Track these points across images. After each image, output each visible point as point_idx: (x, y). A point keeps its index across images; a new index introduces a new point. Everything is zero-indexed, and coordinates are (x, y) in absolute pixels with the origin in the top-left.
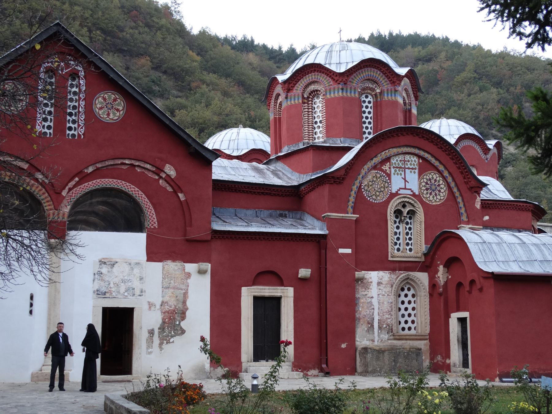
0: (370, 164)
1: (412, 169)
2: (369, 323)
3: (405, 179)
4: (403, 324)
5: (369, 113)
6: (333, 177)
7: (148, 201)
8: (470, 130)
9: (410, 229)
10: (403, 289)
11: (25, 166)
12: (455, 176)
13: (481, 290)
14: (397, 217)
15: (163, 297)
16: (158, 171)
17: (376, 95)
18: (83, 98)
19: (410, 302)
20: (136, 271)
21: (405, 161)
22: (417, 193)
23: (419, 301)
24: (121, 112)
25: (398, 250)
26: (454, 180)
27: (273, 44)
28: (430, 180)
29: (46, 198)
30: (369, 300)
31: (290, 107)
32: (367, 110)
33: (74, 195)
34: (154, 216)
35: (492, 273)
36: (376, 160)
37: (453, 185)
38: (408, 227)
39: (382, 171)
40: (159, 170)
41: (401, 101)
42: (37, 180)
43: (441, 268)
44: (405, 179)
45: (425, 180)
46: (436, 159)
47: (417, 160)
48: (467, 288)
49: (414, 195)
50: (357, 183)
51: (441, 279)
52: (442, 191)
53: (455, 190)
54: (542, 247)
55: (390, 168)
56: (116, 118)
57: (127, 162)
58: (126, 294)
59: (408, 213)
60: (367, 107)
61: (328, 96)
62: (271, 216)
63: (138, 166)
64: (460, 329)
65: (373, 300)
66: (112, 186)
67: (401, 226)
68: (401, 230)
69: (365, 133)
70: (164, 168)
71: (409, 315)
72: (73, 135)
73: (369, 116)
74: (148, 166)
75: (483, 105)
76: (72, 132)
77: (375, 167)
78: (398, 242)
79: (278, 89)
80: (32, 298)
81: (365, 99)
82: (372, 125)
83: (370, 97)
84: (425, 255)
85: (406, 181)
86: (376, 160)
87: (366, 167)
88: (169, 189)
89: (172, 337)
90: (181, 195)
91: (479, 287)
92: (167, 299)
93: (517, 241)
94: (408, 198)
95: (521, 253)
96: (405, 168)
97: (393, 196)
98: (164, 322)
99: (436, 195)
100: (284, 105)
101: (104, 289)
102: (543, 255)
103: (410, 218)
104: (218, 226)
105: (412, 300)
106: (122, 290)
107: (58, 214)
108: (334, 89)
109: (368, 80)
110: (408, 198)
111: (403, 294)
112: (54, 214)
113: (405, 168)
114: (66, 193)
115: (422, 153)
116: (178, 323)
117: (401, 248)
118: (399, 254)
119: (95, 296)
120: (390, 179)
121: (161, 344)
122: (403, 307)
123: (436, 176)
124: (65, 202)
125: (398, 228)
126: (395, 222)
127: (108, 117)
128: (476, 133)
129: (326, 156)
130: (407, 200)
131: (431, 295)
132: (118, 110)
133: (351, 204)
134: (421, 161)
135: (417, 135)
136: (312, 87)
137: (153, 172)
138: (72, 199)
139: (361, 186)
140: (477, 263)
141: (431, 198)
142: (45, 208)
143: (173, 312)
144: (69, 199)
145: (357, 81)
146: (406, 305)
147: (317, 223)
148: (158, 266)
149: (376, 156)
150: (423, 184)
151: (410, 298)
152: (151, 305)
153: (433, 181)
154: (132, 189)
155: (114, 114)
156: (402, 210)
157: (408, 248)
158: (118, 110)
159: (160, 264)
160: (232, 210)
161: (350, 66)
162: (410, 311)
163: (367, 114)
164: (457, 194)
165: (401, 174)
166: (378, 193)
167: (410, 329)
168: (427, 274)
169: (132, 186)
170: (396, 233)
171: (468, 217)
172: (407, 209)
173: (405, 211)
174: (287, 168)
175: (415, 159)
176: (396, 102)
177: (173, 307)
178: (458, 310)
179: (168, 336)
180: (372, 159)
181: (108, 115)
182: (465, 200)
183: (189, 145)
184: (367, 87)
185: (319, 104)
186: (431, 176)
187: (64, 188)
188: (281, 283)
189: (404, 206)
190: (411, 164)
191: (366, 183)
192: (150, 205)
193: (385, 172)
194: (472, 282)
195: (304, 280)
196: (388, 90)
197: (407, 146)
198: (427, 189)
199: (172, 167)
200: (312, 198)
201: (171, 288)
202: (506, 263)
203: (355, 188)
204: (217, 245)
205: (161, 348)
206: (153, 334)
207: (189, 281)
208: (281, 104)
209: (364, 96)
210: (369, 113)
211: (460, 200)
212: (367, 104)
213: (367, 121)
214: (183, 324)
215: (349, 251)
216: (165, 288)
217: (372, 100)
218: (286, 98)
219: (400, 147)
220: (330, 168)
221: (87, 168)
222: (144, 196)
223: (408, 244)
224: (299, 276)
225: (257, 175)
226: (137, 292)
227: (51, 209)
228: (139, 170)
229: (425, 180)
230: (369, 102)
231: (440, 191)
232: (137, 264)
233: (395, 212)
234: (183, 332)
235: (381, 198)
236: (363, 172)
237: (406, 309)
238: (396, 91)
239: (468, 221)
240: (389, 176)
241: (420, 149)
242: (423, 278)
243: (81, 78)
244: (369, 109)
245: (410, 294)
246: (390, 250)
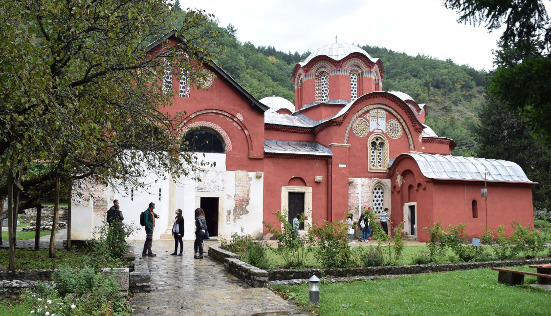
0: (357, 114)
1: (382, 117)
2: (356, 209)
3: (378, 124)
4: (375, 210)
5: (355, 85)
6: (336, 122)
9: (380, 153)
10: (376, 189)
12: (407, 122)
13: (425, 189)
14: (373, 146)
15: (236, 191)
16: (232, 117)
17: (359, 74)
19: (379, 197)
20: (220, 176)
21: (378, 113)
22: (385, 132)
23: (385, 196)
24: (211, 82)
25: (373, 166)
26: (406, 124)
28: (392, 124)
30: (356, 195)
32: (354, 83)
34: (230, 144)
35: (433, 179)
36: (361, 112)
37: (405, 127)
38: (379, 152)
39: (365, 118)
40: (233, 117)
43: (399, 177)
44: (378, 124)
45: (390, 125)
46: (396, 112)
47: (385, 112)
48: (416, 188)
49: (383, 133)
50: (350, 126)
51: (399, 183)
52: (400, 131)
53: (407, 130)
54: (460, 164)
55: (369, 117)
56: (208, 85)
57: (215, 111)
58: (214, 189)
59: (379, 144)
60: (353, 81)
61: (331, 75)
62: (297, 145)
63: (221, 114)
64: (410, 212)
65: (359, 195)
66: (206, 125)
67: (375, 152)
68: (375, 154)
69: (352, 97)
71: (379, 204)
72: (183, 96)
73: (355, 87)
74: (227, 114)
75: (407, 88)
76: (183, 94)
77: (360, 116)
78: (373, 161)
79: (300, 71)
80: (160, 191)
81: (352, 76)
82: (356, 92)
83: (355, 75)
84: (389, 169)
85: (378, 125)
86: (361, 112)
87: (355, 116)
88: (240, 128)
89: (241, 215)
90: (246, 131)
91: (423, 187)
92: (238, 193)
93: (446, 160)
94: (380, 135)
95: (448, 167)
96: (378, 117)
97: (371, 133)
98: (236, 206)
99: (396, 133)
100: (303, 81)
101: (201, 187)
102: (461, 169)
103: (380, 147)
104: (267, 150)
105: (381, 195)
106: (212, 187)
108: (334, 70)
109: (355, 65)
110: (380, 135)
111: (376, 192)
113: (378, 117)
115: (388, 108)
116: (244, 207)
117: (375, 165)
118: (374, 168)
119: (196, 190)
120: (369, 123)
121: (235, 219)
122: (375, 199)
123: (396, 122)
125: (373, 152)
126: (372, 149)
128: (412, 100)
129: (330, 110)
130: (379, 136)
131: (392, 193)
132: (209, 81)
133: (346, 138)
134: (387, 113)
135: (386, 97)
136: (321, 70)
137: (230, 117)
139: (352, 127)
140: (423, 173)
141: (393, 135)
143: (242, 200)
145: (348, 66)
146: (377, 198)
147: (326, 149)
148: (232, 173)
149: (361, 110)
150: (389, 127)
151: (380, 194)
152: (229, 196)
153: (394, 125)
155: (207, 83)
156: (376, 142)
157: (379, 164)
158: (209, 81)
159: (234, 172)
160: (274, 141)
161: (344, 56)
162: (380, 202)
163: (353, 86)
164: (408, 133)
165: (375, 121)
166: (362, 132)
167: (379, 212)
168: (390, 180)
169: (218, 126)
170: (372, 156)
171: (414, 147)
172: (379, 141)
173: (378, 143)
174: (306, 117)
175: (384, 111)
176: (371, 79)
177: (242, 197)
178: (409, 201)
179: (239, 214)
180: (359, 111)
182: (413, 137)
183: (251, 102)
184: (354, 69)
186: (393, 122)
188: (305, 184)
189: (377, 140)
190: (381, 115)
191: (355, 126)
193: (366, 119)
194: (419, 185)
195: (318, 183)
196: (366, 71)
197: (379, 104)
198: (391, 130)
200: (322, 136)
201: (241, 186)
202: (439, 173)
203: (348, 129)
204: (267, 162)
205: (235, 222)
206: (230, 213)
207: (251, 182)
208: (301, 80)
209: (352, 75)
210: (355, 85)
211: (409, 136)
212: (353, 79)
213: (354, 90)
214: (247, 208)
215: (345, 166)
216: (237, 186)
217: (356, 77)
218: (305, 76)
219: (375, 104)
221: (191, 115)
222: (224, 132)
223: (379, 162)
224: (316, 180)
225: (289, 121)
226: (221, 188)
229: (390, 125)
230: (355, 79)
231: (398, 131)
232: (221, 172)
233: (372, 143)
234: (247, 212)
235: (364, 135)
236: (353, 119)
237: (377, 201)
238: (371, 72)
239: (415, 149)
240: (368, 121)
241: (386, 106)
242: (387, 182)
244: (355, 83)
245: (381, 191)
246: (369, 166)
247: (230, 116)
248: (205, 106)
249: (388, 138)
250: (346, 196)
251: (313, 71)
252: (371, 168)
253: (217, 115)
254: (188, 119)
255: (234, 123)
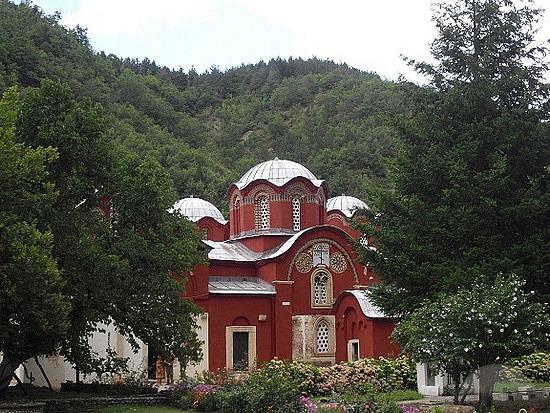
8: (361, 205)
13: (365, 327)
27: (173, 66)
31: (245, 206)
37: (350, 260)
41: (317, 202)
136: (261, 194)
145: (290, 192)
161: (286, 181)
185: (265, 205)
194: (361, 322)
215: (288, 304)
220: (275, 252)
242: (332, 318)
249: (331, 272)
250: (290, 335)
251: (253, 192)
252: (315, 304)
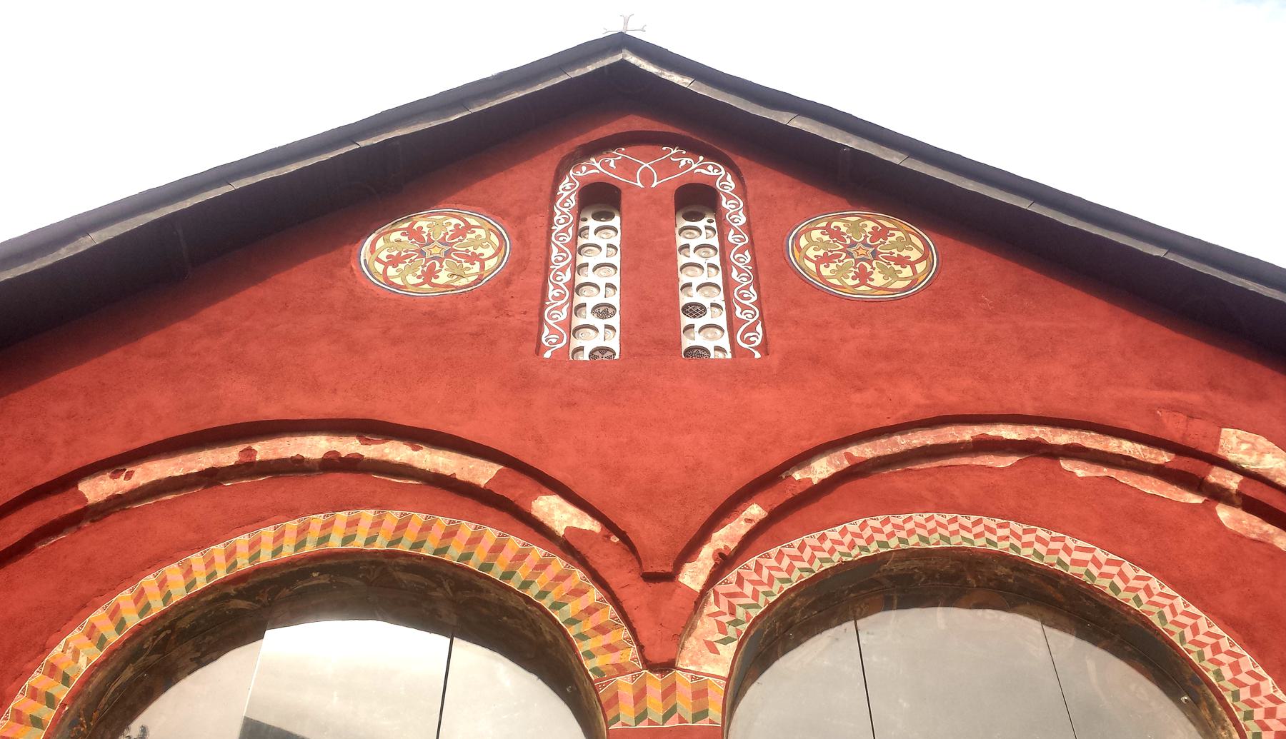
7: (1193, 609)
11: (482, 472)
16: (1186, 464)
18: (740, 244)
29: (590, 611)
33: (748, 589)
42: (540, 530)
70: (1217, 444)
107: (669, 692)
112: (640, 695)
114: (703, 578)
124: (706, 626)
127: (863, 283)
138: (740, 612)
142: (589, 665)
144: (724, 607)
154: (1077, 555)
181: (863, 276)
187: (689, 552)
192: (1216, 630)
199: (1262, 440)
227: (621, 670)
228: (1080, 473)
243: (726, 194)
247: (1164, 458)
248: (913, 398)
253: (1043, 463)
254: (776, 496)
255: (1224, 513)
